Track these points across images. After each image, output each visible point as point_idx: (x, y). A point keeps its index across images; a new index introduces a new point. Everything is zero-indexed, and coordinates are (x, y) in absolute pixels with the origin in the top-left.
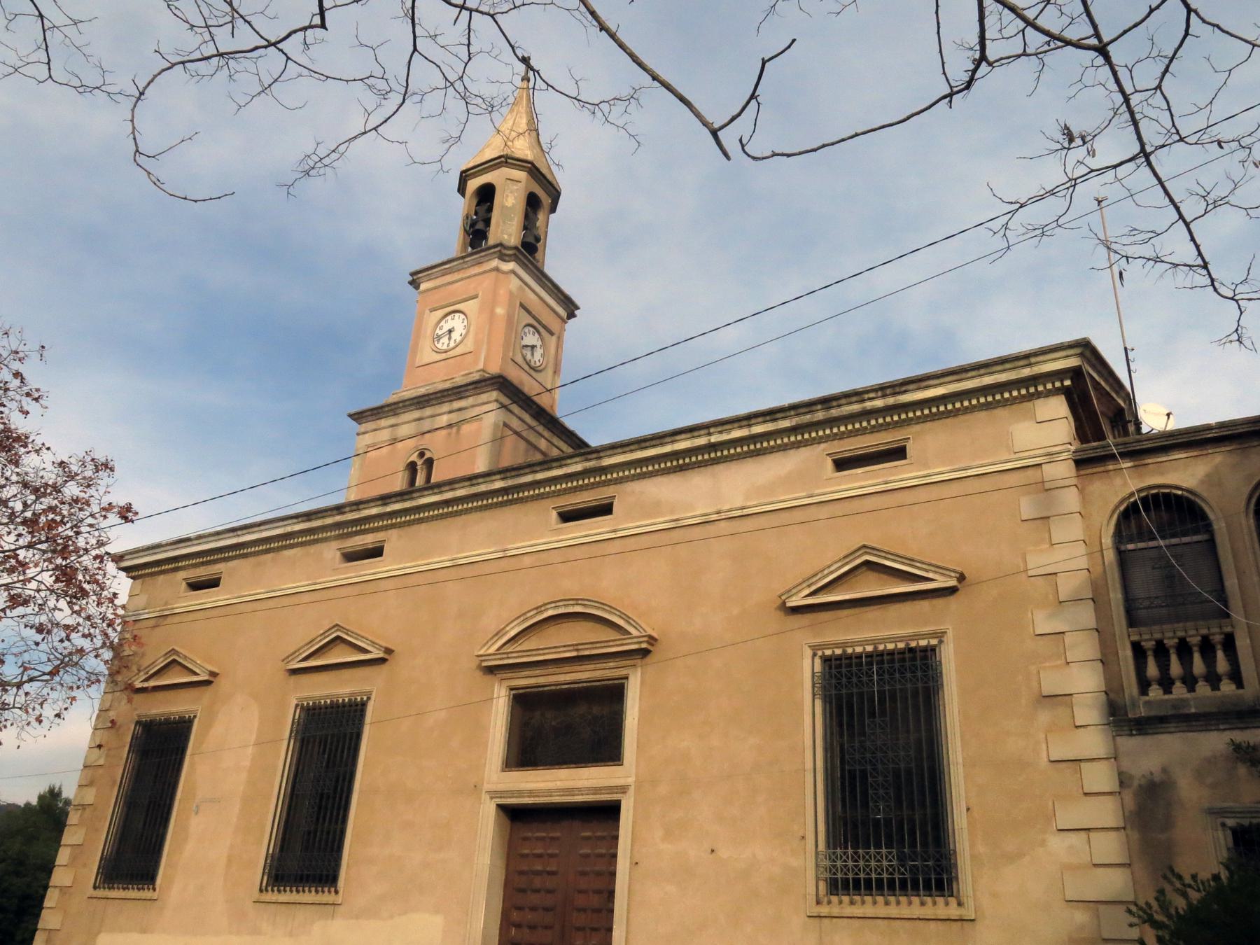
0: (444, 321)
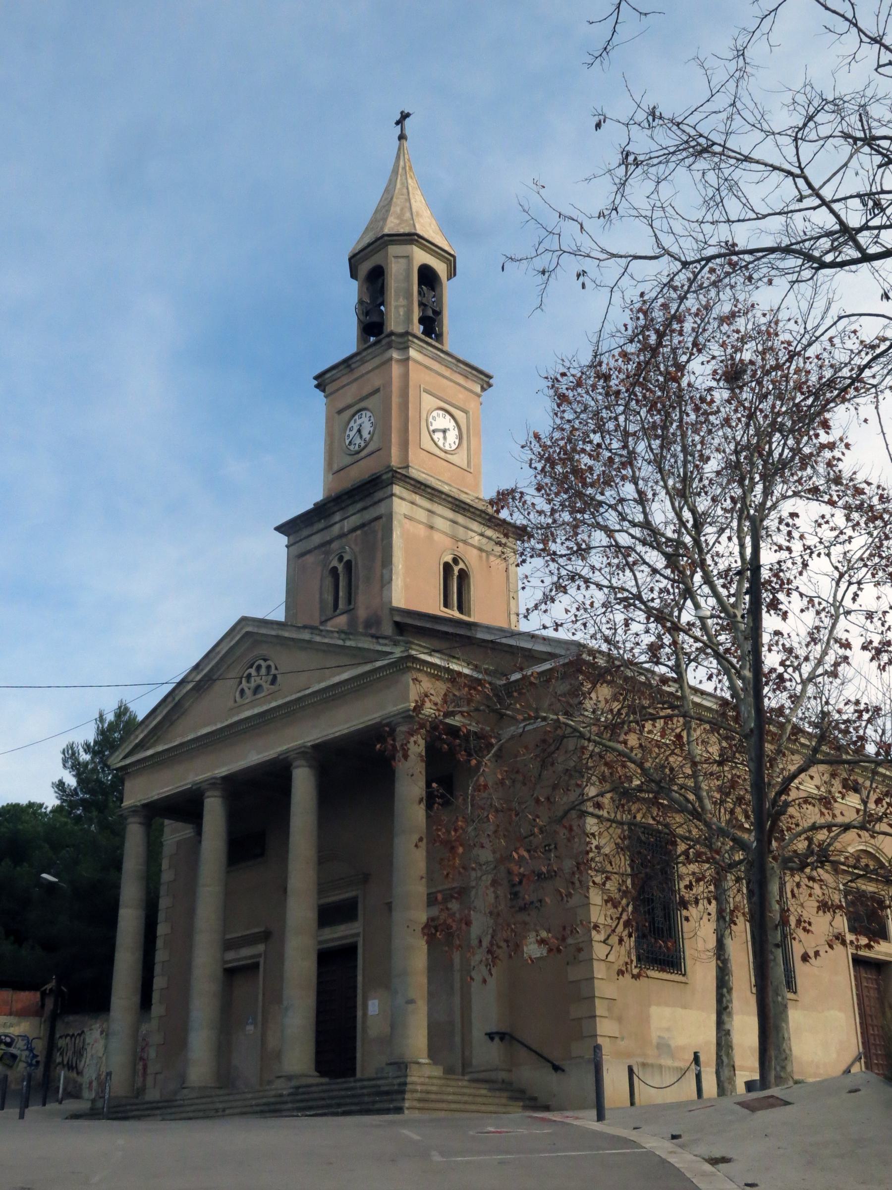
0: (353, 421)
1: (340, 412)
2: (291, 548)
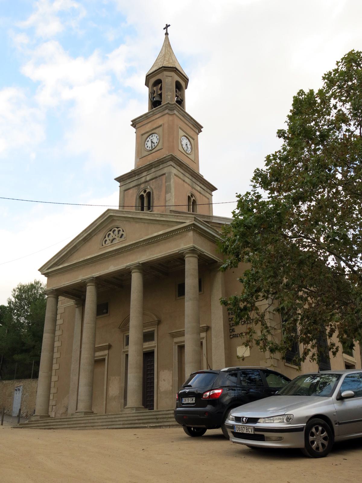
0: (148, 138)
1: (142, 135)
2: (121, 187)
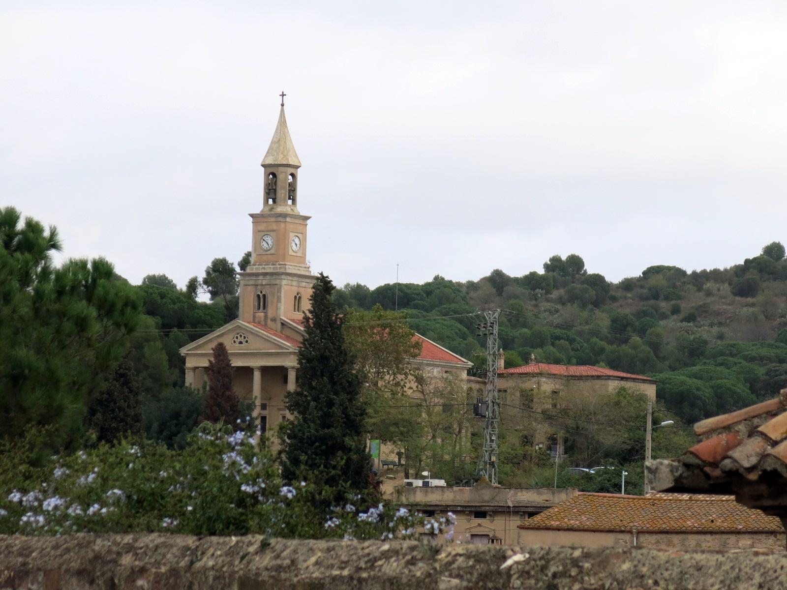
1: (259, 231)
